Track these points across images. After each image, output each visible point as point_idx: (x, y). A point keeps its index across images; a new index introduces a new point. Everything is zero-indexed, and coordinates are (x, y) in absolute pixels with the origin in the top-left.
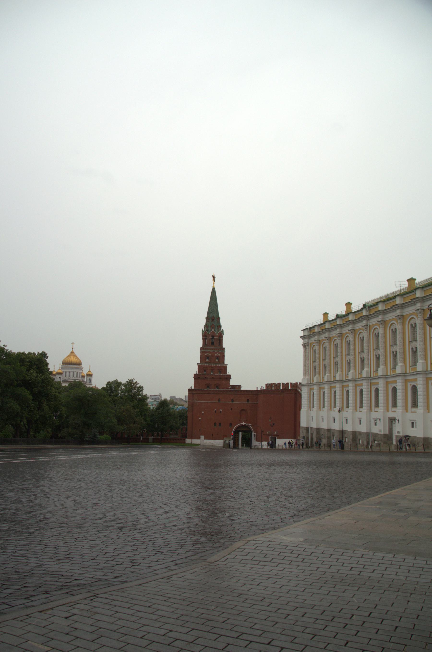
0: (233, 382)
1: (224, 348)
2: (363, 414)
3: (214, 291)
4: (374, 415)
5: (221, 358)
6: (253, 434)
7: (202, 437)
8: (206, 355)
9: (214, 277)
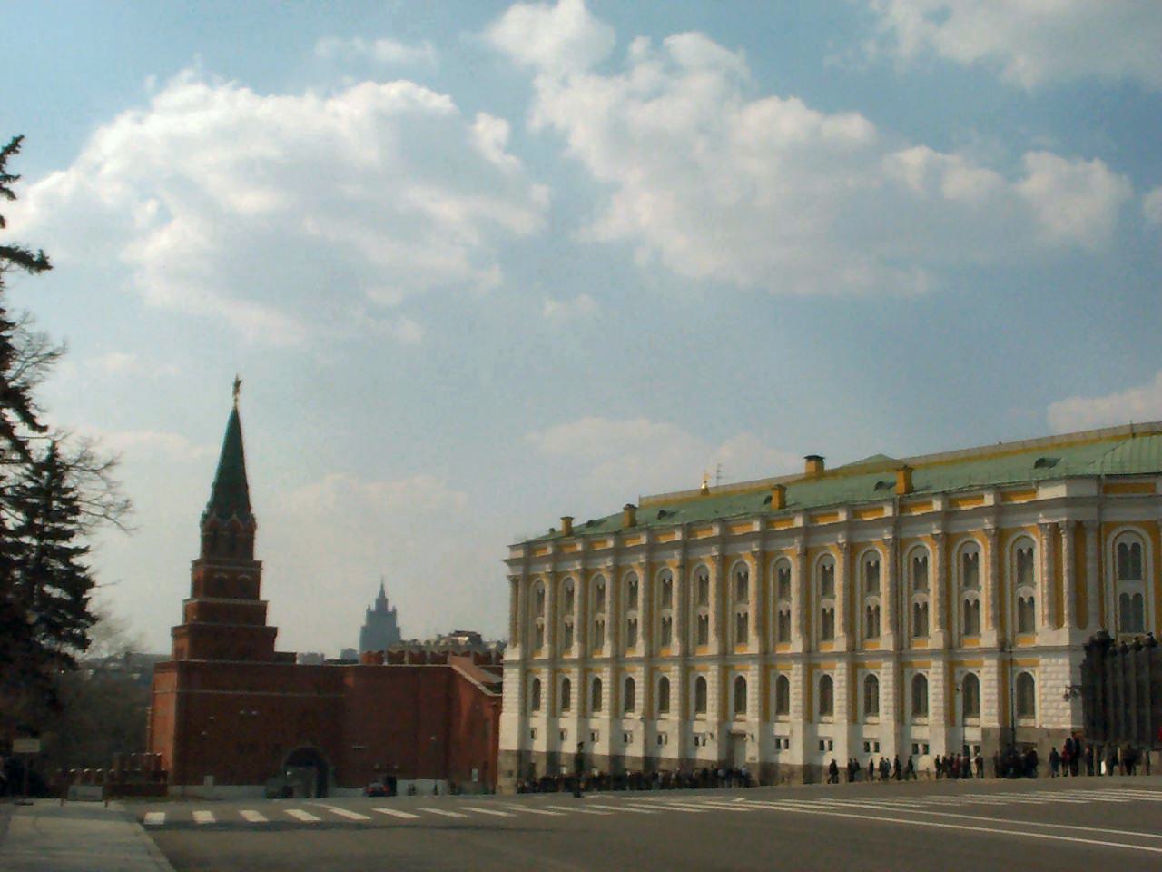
0: (281, 645)
6: (332, 769)
7: (209, 779)
8: (217, 576)
9: (237, 384)
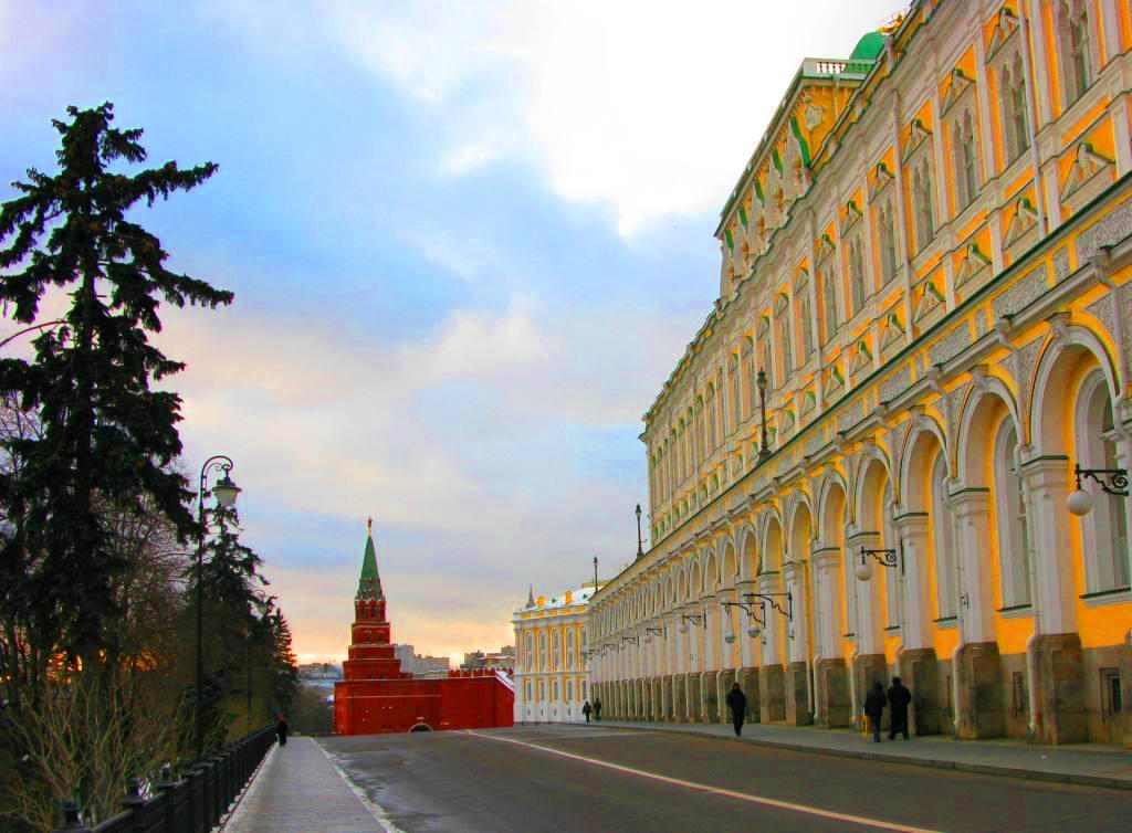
1: (388, 624)
2: (558, 704)
3: (370, 542)
4: (554, 705)
5: (385, 635)
9: (370, 522)
